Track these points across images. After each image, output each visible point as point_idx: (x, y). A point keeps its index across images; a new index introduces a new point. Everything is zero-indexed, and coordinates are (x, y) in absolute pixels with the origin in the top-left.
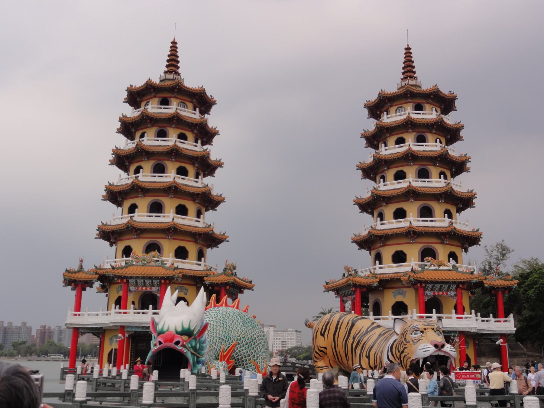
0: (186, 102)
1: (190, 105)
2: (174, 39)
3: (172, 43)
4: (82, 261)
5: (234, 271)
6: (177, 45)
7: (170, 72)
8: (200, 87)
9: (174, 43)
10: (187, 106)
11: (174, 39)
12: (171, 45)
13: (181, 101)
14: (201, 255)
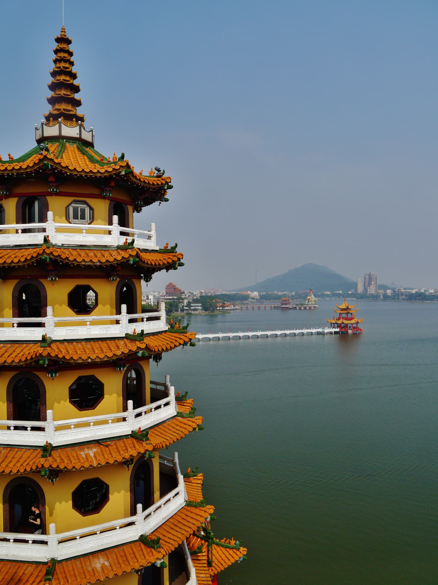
0: (89, 201)
1: (101, 207)
2: (63, 30)
3: (58, 40)
6: (71, 48)
7: (51, 118)
8: (119, 156)
9: (63, 40)
10: (91, 209)
11: (63, 30)
12: (55, 45)
13: (71, 199)
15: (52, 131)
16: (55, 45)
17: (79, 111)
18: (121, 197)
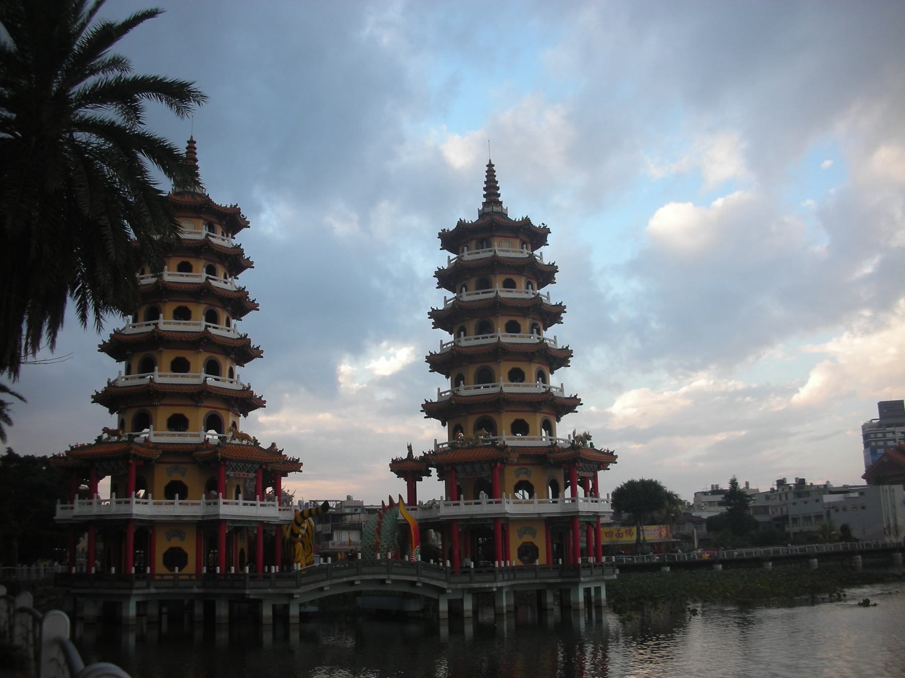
1: (517, 242)
4: (410, 448)
5: (588, 442)
6: (494, 168)
9: (490, 165)
14: (549, 427)
15: (487, 210)
16: (487, 169)
17: (500, 199)
18: (527, 240)
